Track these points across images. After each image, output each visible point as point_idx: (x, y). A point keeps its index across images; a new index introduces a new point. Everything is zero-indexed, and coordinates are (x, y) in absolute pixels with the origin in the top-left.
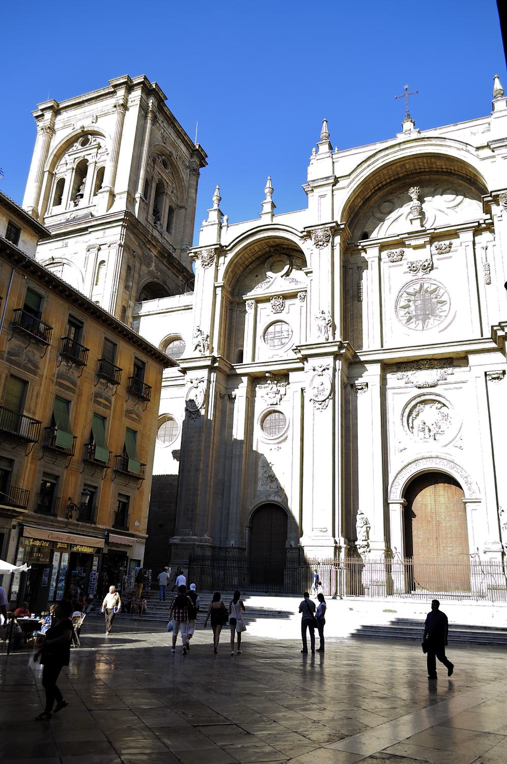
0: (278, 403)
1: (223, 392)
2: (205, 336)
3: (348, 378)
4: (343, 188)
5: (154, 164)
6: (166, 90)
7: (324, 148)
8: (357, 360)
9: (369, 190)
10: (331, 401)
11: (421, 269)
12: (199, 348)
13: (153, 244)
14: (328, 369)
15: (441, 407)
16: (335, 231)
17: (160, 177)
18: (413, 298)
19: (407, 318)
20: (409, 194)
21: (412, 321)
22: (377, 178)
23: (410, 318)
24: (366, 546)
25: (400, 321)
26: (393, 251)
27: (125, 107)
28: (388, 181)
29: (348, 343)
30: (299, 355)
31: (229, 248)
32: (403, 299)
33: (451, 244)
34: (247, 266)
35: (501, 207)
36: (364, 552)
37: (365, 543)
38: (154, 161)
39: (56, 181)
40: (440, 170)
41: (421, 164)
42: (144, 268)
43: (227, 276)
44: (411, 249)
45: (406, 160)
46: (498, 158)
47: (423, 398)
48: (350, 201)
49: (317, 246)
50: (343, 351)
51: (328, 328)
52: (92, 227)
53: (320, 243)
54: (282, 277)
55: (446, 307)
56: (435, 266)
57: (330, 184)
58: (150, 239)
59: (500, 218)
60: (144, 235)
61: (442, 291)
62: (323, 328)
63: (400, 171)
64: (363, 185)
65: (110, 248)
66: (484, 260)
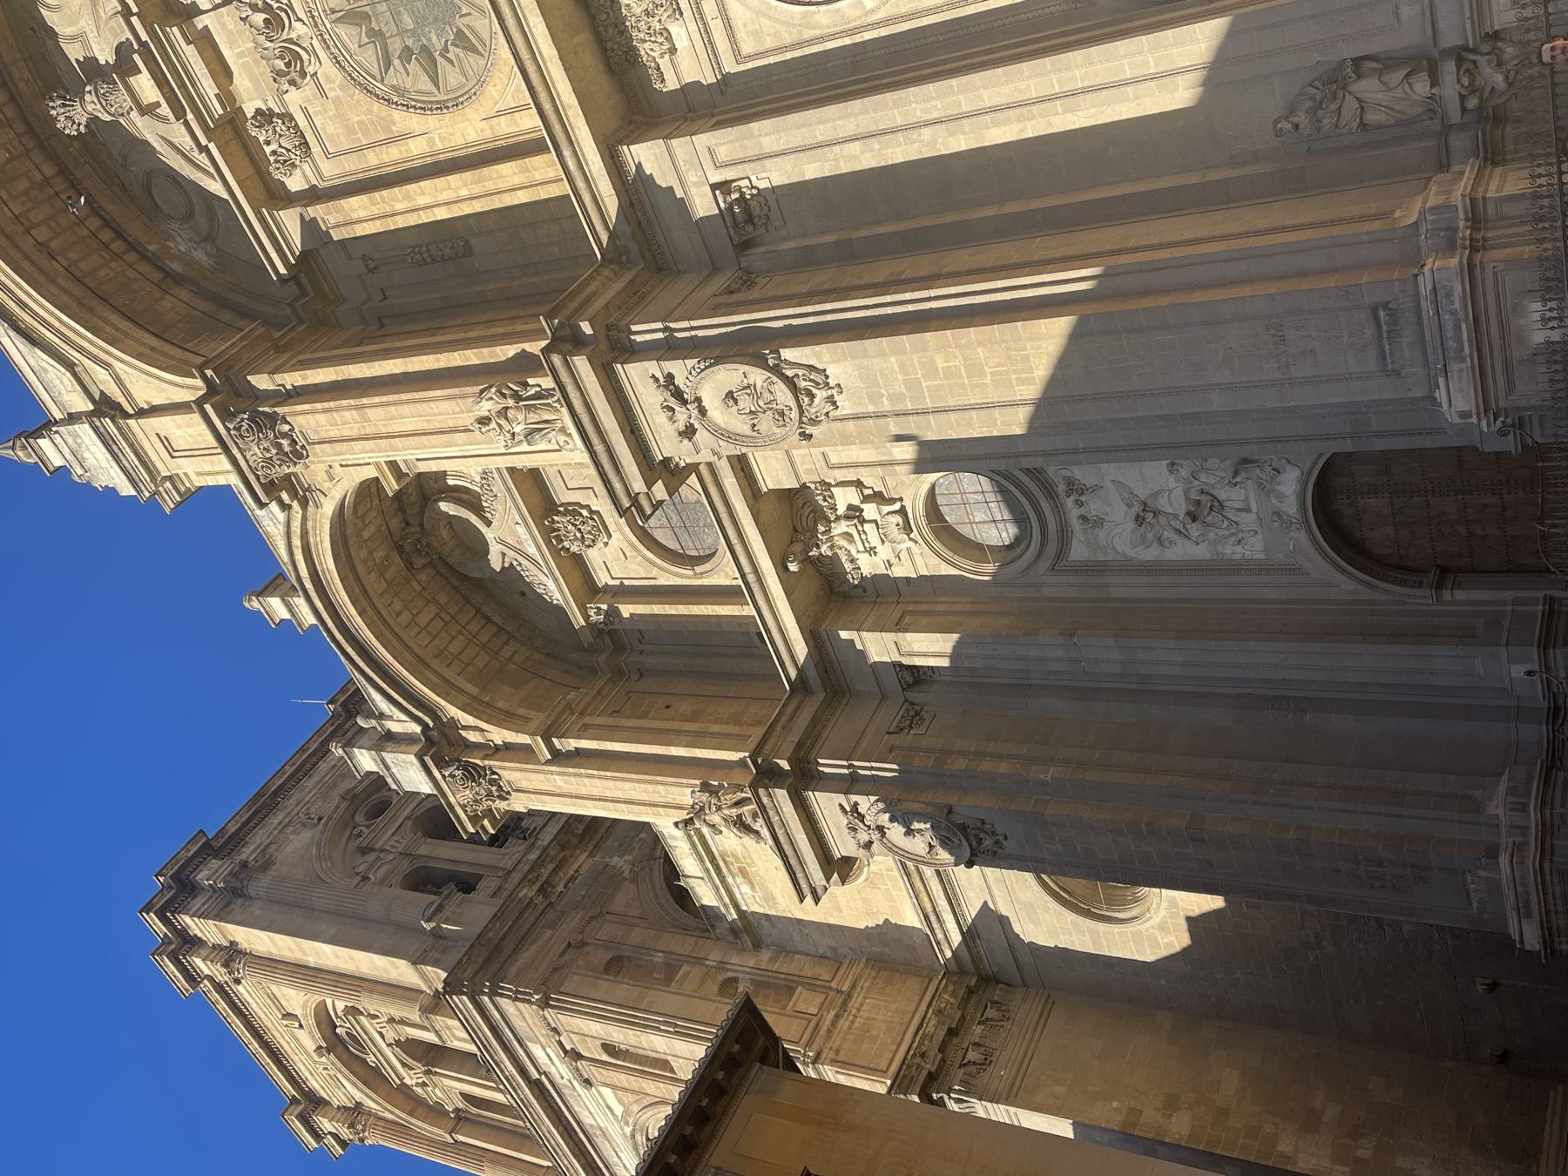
0: (897, 506)
1: (890, 715)
2: (705, 797)
3: (716, 269)
4: (118, 380)
5: (373, 850)
6: (175, 843)
7: (51, 451)
8: (634, 247)
9: (130, 273)
10: (788, 354)
11: (285, 36)
12: (749, 820)
13: (555, 871)
14: (670, 377)
16: (239, 395)
17: (409, 824)
18: (396, 46)
20: (82, 129)
22: (73, 256)
23: (461, 39)
24: (1460, 61)
25: (481, 83)
27: (231, 955)
29: (549, 317)
30: (659, 491)
31: (431, 724)
32: (408, 83)
34: (500, 628)
36: (1500, 64)
37: (1449, 67)
38: (364, 851)
39: (474, 1110)
42: (619, 903)
43: (521, 711)
44: (242, 84)
48: (153, 349)
49: (300, 456)
50: (586, 328)
51: (532, 392)
52: (523, 1072)
53: (287, 449)
54: (489, 523)
57: (119, 429)
58: (537, 886)
60: (521, 913)
62: (533, 417)
63: (30, 179)
64: (91, 310)
65: (560, 1029)
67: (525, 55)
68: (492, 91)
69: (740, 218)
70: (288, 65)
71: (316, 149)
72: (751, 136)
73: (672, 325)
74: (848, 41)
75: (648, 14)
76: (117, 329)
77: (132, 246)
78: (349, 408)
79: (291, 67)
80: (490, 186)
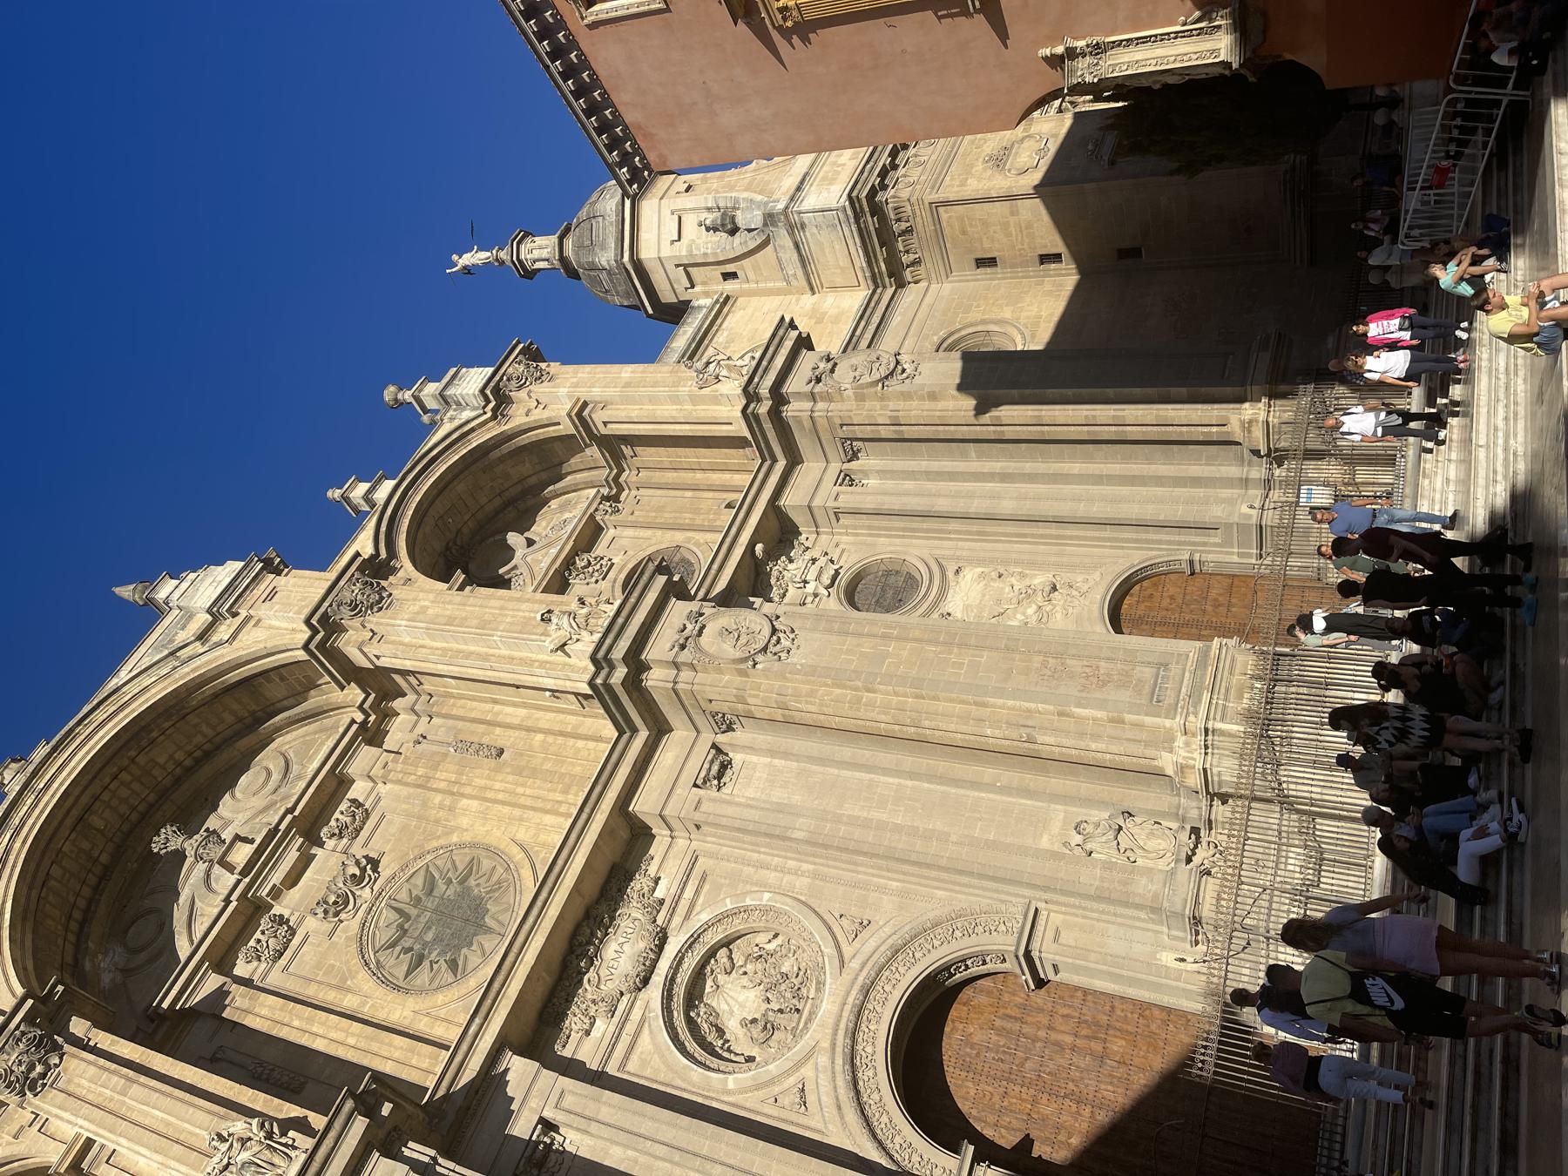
9: (60, 941)
15: (730, 958)
18: (407, 942)
19: (444, 966)
21: (460, 963)
22: (51, 898)
26: (252, 943)
28: (87, 891)
33: (354, 801)
35: (356, 622)
40: (178, 770)
41: (124, 793)
44: (294, 895)
45: (78, 798)
46: (262, 611)
47: (680, 991)
48: (25, 969)
50: (386, 1109)
51: (283, 1140)
55: (486, 864)
56: (373, 855)
59: (377, 638)
61: (438, 862)
62: (267, 1154)
64: (24, 919)
66: (443, 750)
67: (515, 949)
68: (440, 998)
69: (538, 1155)
70: (335, 903)
71: (282, 962)
72: (597, 1100)
73: (440, 1160)
74: (700, 1100)
75: (594, 1001)
76: (23, 942)
77: (81, 936)
78: (122, 1076)
79: (335, 907)
80: (375, 1047)
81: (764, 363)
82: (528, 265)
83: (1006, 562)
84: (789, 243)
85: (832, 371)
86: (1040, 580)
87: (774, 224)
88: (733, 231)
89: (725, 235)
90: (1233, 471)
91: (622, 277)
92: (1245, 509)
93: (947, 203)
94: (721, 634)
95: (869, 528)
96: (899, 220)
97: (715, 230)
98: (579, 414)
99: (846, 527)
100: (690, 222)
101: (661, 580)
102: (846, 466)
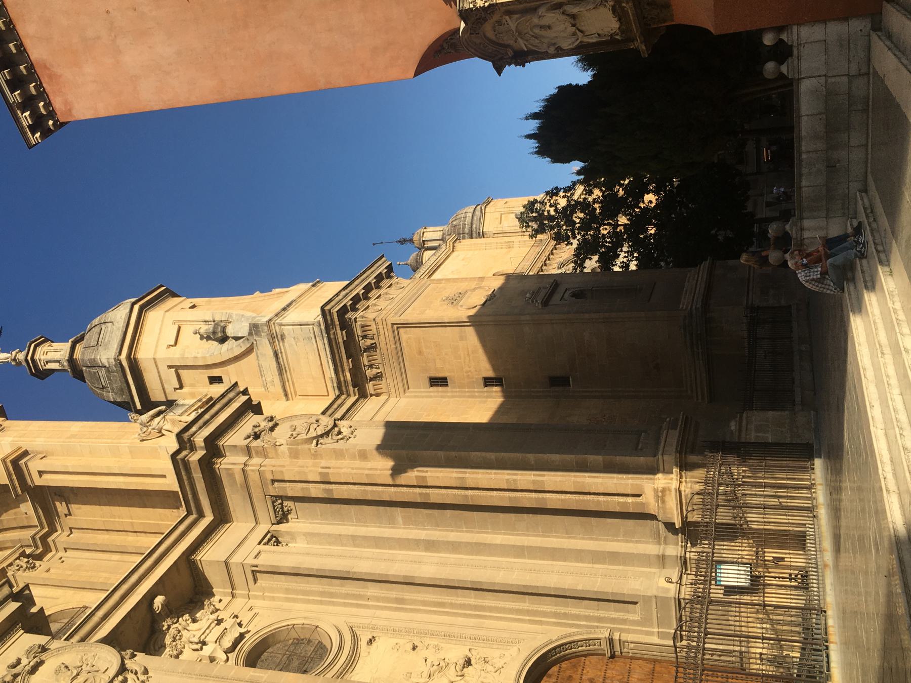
81: (207, 417)
82: (41, 365)
83: (423, 634)
84: (270, 353)
85: (272, 429)
86: (456, 653)
87: (258, 333)
88: (223, 339)
89: (215, 343)
90: (652, 549)
91: (117, 375)
92: (663, 583)
93: (406, 325)
94: (57, 672)
95: (287, 591)
96: (364, 337)
97: (208, 338)
98: (15, 462)
99: (263, 589)
100: (187, 331)
101: (13, 606)
102: (275, 527)
